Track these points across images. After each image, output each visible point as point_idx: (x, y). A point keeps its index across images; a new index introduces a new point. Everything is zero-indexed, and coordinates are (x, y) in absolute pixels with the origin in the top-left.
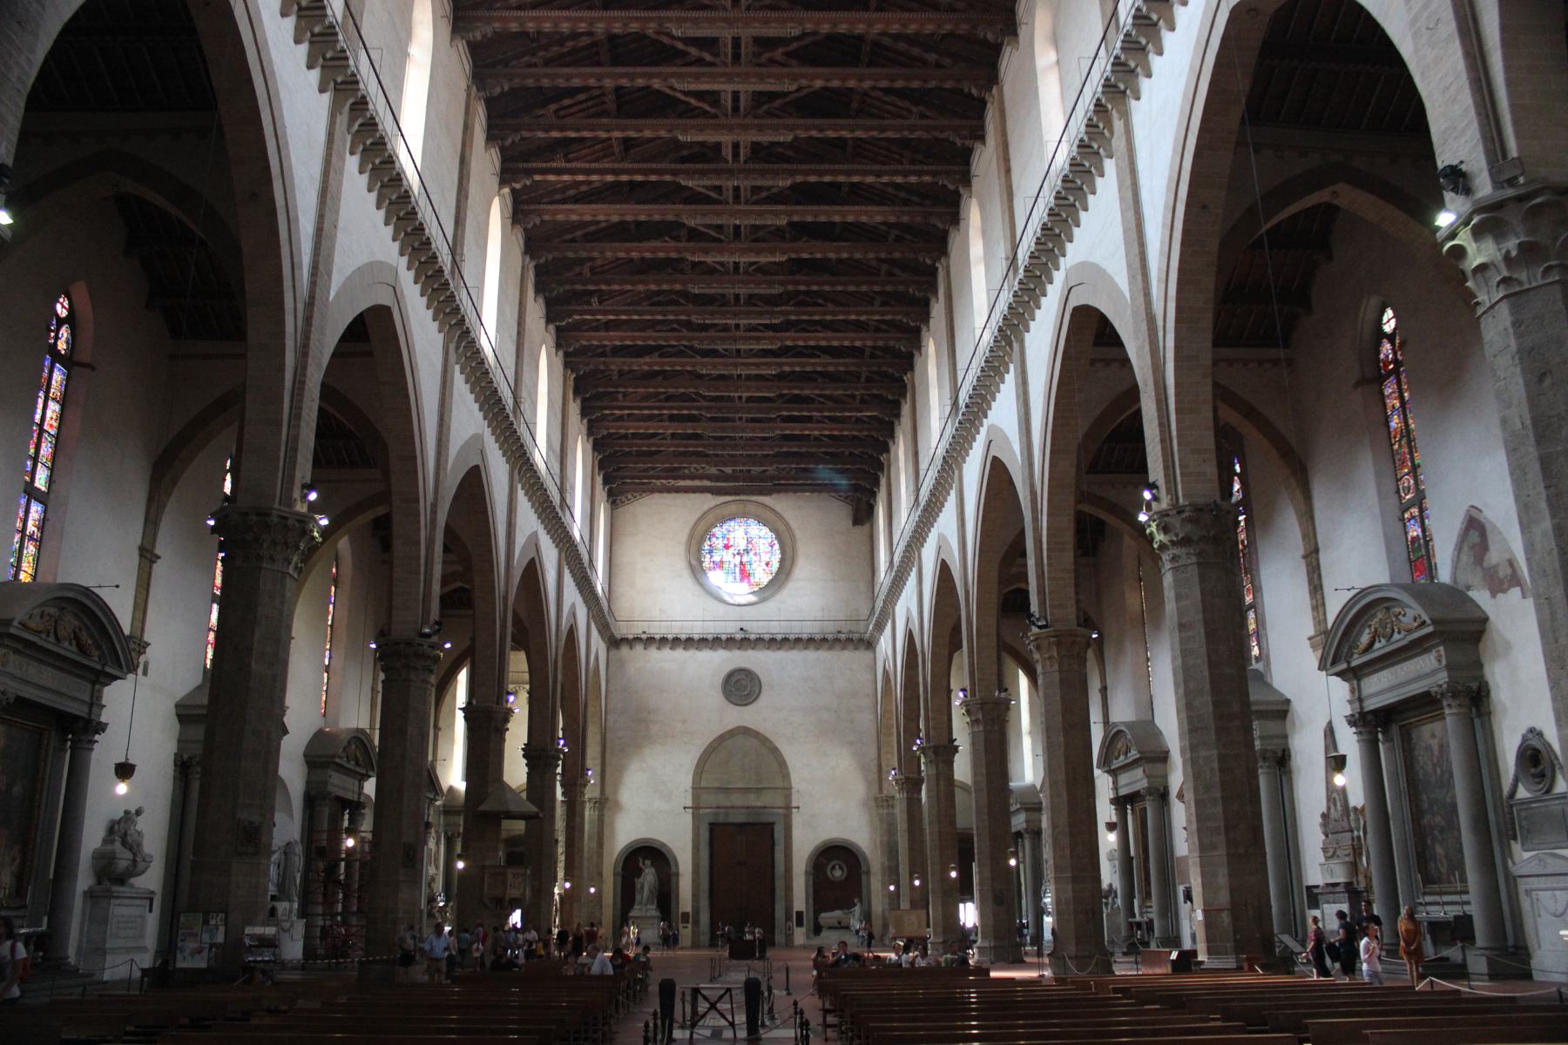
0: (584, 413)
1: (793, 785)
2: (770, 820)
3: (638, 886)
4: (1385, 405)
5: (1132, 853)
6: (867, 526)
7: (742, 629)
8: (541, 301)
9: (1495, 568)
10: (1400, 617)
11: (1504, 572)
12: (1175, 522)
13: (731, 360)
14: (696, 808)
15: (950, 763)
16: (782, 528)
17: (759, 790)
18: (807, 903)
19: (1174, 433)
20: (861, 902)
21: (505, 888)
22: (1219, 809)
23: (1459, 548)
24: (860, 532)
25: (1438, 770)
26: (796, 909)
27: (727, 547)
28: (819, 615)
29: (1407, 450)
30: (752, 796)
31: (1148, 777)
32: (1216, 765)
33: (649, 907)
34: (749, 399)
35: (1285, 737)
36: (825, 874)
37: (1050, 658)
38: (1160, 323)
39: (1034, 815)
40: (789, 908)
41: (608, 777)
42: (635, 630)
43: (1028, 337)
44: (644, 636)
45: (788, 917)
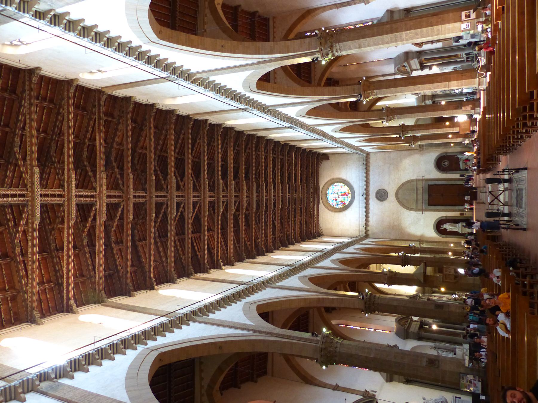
0: (293, 244)
2: (427, 186)
3: (450, 230)
5: (441, 62)
6: (330, 156)
8: (258, 257)
12: (324, 52)
13: (277, 198)
14: (423, 210)
15: (408, 126)
16: (330, 182)
17: (417, 190)
19: (295, 53)
20: (457, 155)
21: (450, 274)
24: (331, 158)
27: (336, 200)
28: (358, 170)
30: (419, 192)
32: (408, 32)
33: (458, 226)
34: (289, 192)
35: (400, 10)
38: (260, 60)
39: (427, 97)
40: (459, 180)
41: (412, 239)
42: (363, 229)
44: (365, 226)
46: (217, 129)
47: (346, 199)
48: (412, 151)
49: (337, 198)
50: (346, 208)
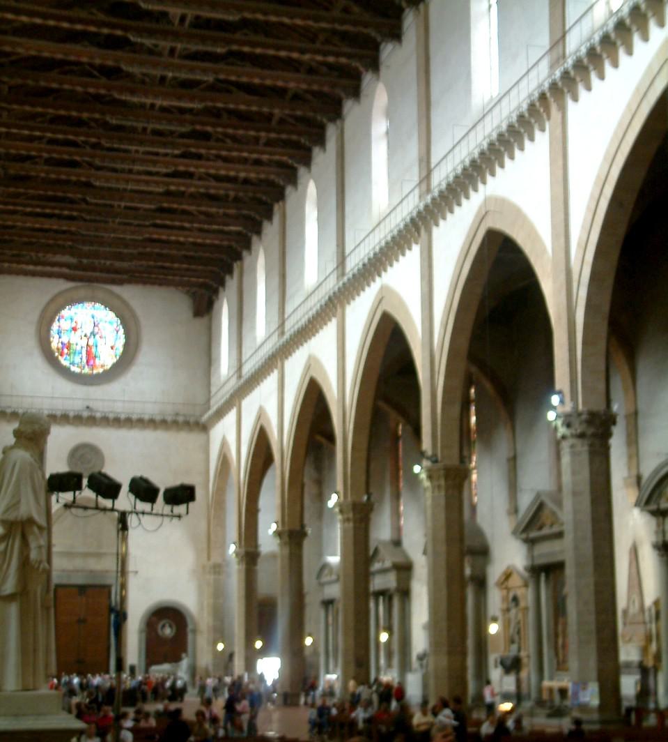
6: (204, 320)
7: (88, 407)
18: (140, 656)
24: (200, 323)
27: (74, 329)
34: (126, 208)
38: (575, 276)
43: (435, 230)
47: (77, 360)
48: (205, 546)
49: (79, 332)
50: (51, 358)
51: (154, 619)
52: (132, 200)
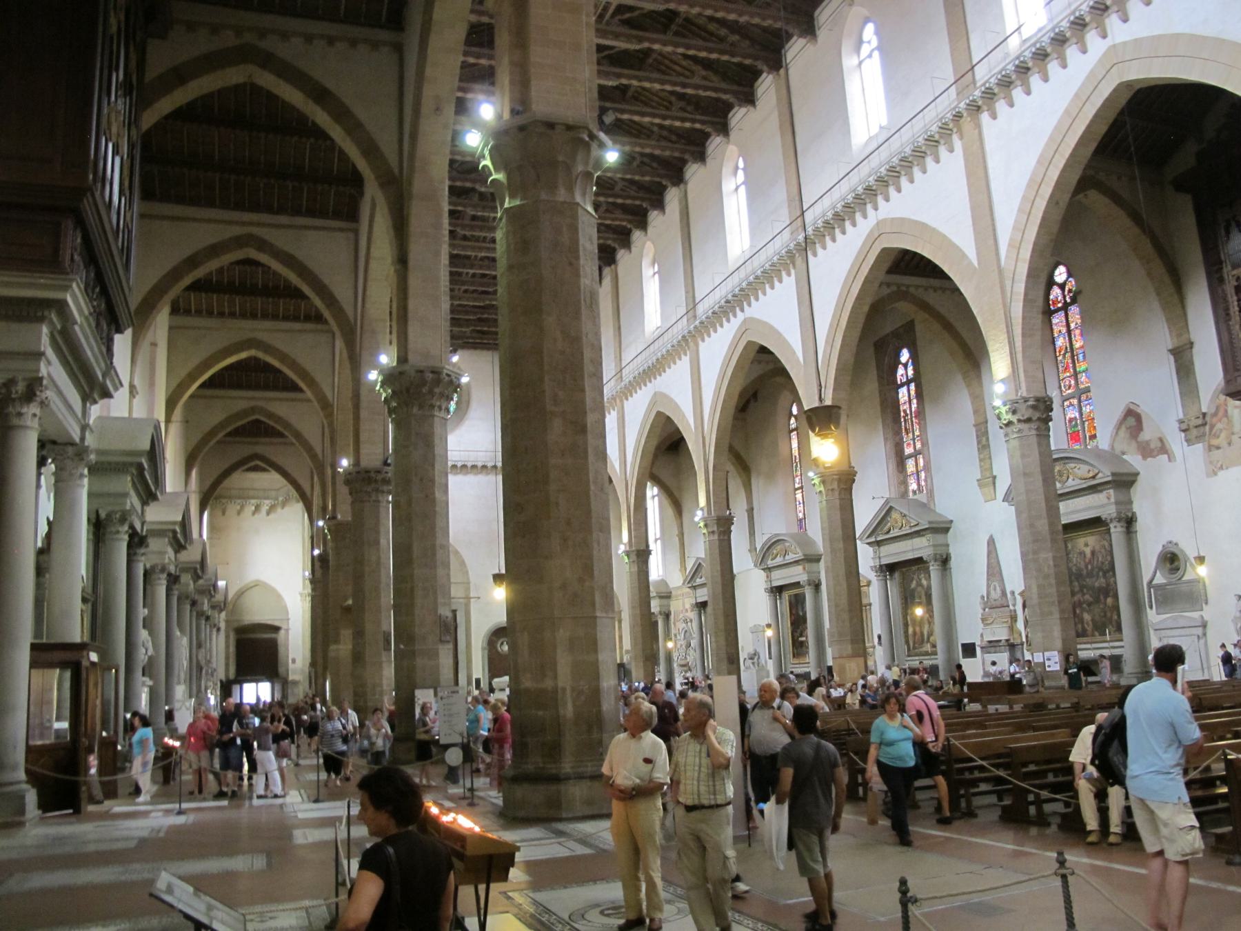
1: (471, 580)
4: (1052, 330)
9: (1148, 443)
10: (1076, 470)
11: (1155, 444)
12: (1022, 407)
22: (1054, 590)
23: (1118, 428)
25: (1090, 567)
26: (475, 677)
29: (1070, 361)
31: (808, 573)
32: (1051, 563)
34: (474, 275)
36: (495, 648)
37: (833, 490)
39: (665, 602)
45: (469, 683)
46: (717, 123)
51: (494, 638)
52: (481, 267)
